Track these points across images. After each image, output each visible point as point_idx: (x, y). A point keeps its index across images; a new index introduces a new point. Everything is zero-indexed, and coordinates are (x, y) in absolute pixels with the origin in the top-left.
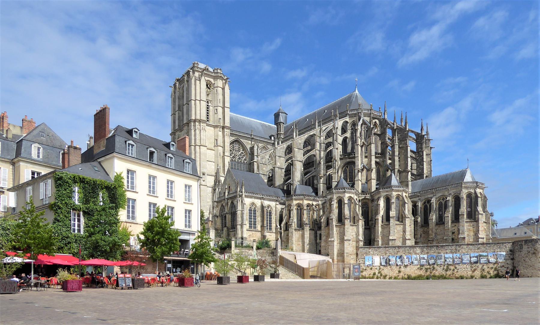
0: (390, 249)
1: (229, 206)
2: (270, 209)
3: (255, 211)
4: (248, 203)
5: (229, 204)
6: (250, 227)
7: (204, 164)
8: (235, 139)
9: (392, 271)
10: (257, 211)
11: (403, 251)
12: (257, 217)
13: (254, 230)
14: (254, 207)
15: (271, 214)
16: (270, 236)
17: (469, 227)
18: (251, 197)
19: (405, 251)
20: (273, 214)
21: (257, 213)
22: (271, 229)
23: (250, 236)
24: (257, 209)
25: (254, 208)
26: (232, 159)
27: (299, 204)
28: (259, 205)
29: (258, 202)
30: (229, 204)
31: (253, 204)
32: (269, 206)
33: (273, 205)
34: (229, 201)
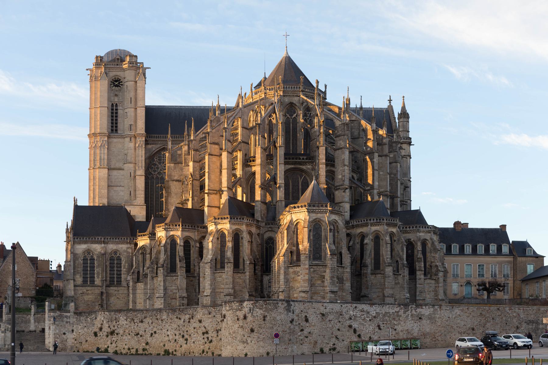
0: (138, 313)
3: (92, 259)
6: (85, 281)
7: (103, 192)
8: (160, 147)
9: (139, 343)
11: (150, 316)
12: (95, 268)
13: (91, 285)
14: (91, 255)
15: (121, 262)
16: (116, 292)
17: (293, 274)
18: (85, 243)
19: (151, 316)
20: (123, 261)
21: (96, 263)
22: (119, 283)
23: (83, 294)
26: (158, 175)
27: (144, 246)
28: (98, 252)
29: (97, 248)
31: (88, 251)
32: (115, 252)
33: (123, 249)
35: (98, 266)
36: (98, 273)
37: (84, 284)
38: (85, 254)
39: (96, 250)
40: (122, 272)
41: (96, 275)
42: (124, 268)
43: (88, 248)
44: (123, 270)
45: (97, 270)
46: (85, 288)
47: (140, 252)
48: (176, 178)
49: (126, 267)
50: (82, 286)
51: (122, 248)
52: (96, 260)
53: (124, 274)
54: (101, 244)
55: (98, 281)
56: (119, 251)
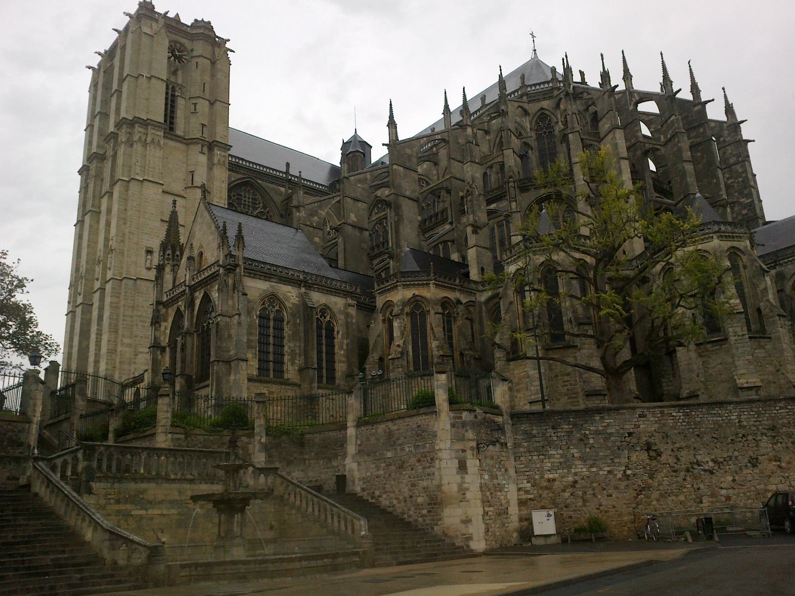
1: (197, 308)
2: (328, 318)
3: (279, 320)
4: (258, 294)
5: (198, 302)
10: (285, 323)
12: (285, 341)
20: (338, 332)
21: (286, 329)
24: (285, 313)
25: (277, 311)
28: (293, 304)
30: (198, 302)
31: (272, 298)
34: (197, 294)
35: (294, 337)
36: (293, 354)
37: (260, 375)
38: (263, 304)
39: (288, 299)
40: (337, 358)
41: (286, 358)
42: (341, 348)
43: (271, 290)
44: (340, 353)
45: (291, 345)
46: (265, 385)
47: (407, 310)
48: (408, 193)
49: (345, 347)
50: (261, 381)
51: (336, 304)
52: (288, 322)
53: (341, 362)
54: (299, 286)
55: (291, 372)
56: (330, 310)
